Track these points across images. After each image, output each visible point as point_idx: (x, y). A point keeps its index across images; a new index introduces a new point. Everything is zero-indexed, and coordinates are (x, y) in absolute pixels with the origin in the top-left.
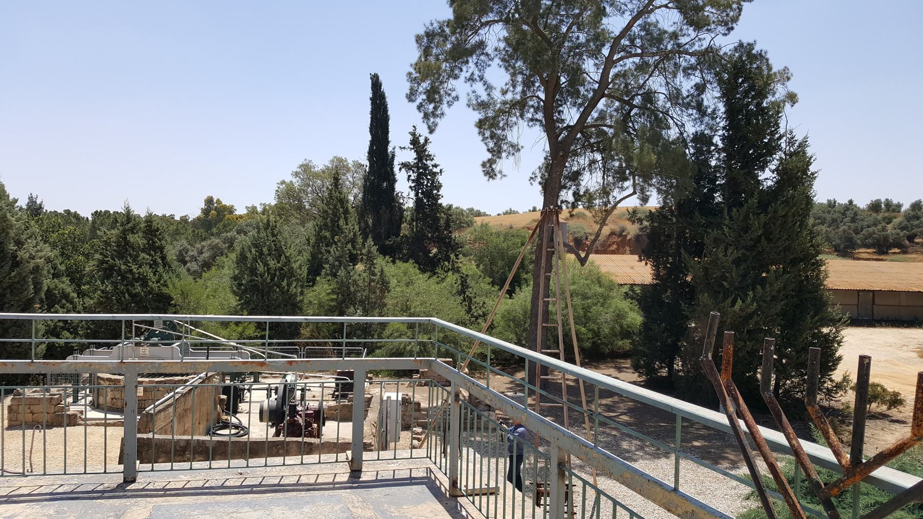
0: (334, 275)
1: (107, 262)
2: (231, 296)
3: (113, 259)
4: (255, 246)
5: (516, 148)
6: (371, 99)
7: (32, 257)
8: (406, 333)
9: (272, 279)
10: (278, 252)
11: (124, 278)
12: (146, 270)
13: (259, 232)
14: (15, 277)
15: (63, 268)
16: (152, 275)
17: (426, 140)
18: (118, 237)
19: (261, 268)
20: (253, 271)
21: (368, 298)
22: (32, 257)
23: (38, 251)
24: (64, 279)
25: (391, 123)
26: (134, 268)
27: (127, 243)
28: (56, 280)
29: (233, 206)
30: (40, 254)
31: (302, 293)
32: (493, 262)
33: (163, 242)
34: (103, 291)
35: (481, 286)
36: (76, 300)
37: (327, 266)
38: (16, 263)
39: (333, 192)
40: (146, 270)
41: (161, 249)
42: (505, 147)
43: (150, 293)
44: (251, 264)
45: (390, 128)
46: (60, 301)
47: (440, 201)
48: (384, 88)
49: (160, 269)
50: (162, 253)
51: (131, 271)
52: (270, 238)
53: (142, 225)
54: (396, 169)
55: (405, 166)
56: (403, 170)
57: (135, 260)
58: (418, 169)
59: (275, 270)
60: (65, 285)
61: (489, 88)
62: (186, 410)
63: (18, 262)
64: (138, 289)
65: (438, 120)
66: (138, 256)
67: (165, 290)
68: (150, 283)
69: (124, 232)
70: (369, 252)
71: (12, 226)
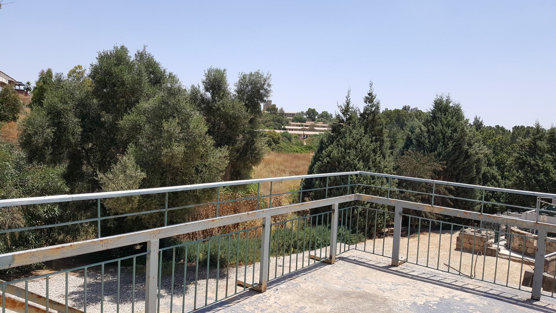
1: (522, 159)
11: (532, 169)
15: (494, 160)
23: (480, 150)
24: (494, 167)
26: (540, 163)
27: (536, 146)
28: (489, 168)
30: (481, 152)
34: (517, 177)
36: (501, 181)
38: (467, 156)
43: (550, 180)
46: (490, 181)
51: (537, 165)
57: (541, 157)
60: (494, 171)
64: (542, 177)
66: (542, 156)
68: (551, 174)
69: (534, 140)
71: (467, 135)
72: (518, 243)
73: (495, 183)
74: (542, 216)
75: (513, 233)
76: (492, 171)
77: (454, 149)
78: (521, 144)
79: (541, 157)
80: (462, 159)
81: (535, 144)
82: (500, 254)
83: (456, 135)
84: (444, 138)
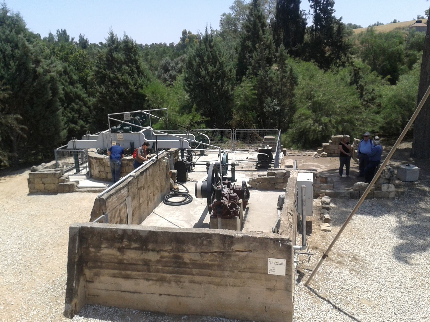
0: (256, 75)
1: (101, 72)
2: (184, 92)
4: (199, 55)
7: (49, 71)
8: (311, 116)
9: (211, 80)
10: (214, 60)
11: (113, 83)
13: (200, 45)
14: (36, 85)
15: (75, 77)
16: (131, 80)
18: (108, 54)
19: (203, 73)
20: (198, 74)
21: (281, 90)
26: (119, 76)
27: (113, 58)
28: (71, 87)
31: (232, 89)
32: (376, 57)
33: (137, 57)
34: (101, 93)
35: (369, 77)
38: (36, 76)
39: (253, 11)
41: (136, 61)
44: (196, 70)
47: (333, 15)
49: (136, 76)
50: (136, 64)
51: (117, 78)
52: (209, 49)
53: (122, 46)
57: (119, 69)
59: (213, 73)
60: (79, 90)
62: (139, 189)
63: (37, 75)
66: (121, 67)
67: (140, 91)
68: (130, 86)
70: (281, 55)
72: (97, 170)
73: (80, 102)
74: (118, 134)
75: (91, 159)
78: (99, 55)
79: (119, 69)
80: (30, 80)
81: (111, 56)
82: (79, 188)
84: (4, 57)
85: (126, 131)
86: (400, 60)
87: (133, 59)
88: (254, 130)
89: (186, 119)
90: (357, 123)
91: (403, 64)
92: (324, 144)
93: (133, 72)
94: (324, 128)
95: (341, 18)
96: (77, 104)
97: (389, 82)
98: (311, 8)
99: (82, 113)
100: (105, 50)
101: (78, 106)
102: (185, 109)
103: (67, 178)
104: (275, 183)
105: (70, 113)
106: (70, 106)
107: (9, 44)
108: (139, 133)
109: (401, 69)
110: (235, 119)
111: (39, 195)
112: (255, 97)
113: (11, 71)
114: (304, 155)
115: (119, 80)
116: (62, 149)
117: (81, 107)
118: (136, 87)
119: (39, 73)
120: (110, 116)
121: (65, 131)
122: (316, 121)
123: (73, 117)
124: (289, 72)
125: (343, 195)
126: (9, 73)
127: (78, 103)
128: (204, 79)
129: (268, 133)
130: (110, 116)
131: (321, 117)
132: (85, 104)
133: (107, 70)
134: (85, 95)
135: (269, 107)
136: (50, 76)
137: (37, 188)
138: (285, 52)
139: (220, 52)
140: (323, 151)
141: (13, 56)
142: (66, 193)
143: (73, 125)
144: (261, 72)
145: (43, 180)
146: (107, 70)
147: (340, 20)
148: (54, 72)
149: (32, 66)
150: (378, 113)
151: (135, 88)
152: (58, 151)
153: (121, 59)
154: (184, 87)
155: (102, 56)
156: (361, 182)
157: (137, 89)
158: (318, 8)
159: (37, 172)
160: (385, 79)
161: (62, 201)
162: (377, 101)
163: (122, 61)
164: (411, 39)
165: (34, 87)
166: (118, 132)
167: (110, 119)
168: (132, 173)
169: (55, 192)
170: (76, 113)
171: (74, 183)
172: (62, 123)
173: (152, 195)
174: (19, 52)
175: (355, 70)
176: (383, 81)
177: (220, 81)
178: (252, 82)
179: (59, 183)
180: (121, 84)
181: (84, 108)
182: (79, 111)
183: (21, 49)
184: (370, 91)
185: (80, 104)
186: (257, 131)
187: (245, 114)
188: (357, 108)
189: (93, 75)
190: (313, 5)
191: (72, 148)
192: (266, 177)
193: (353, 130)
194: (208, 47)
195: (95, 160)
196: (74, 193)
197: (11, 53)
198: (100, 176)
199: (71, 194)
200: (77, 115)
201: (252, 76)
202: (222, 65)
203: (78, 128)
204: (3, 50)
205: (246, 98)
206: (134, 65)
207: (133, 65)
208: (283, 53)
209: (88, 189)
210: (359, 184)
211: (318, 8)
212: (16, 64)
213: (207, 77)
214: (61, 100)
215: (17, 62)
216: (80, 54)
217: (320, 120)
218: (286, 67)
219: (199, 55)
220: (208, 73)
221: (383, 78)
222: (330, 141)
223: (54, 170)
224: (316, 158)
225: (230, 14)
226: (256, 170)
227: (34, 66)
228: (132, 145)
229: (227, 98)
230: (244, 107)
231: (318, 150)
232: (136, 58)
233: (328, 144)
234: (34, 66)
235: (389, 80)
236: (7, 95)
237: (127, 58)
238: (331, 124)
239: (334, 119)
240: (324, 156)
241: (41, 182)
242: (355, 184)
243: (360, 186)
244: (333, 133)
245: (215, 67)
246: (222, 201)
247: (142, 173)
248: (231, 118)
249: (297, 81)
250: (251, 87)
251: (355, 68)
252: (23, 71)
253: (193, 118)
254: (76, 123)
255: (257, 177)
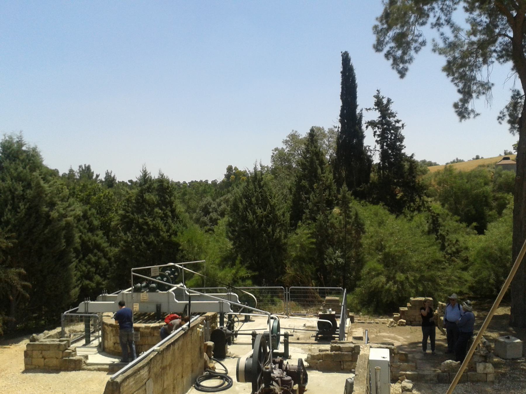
0: (314, 220)
1: (128, 217)
3: (133, 214)
5: (486, 87)
6: (341, 72)
7: (65, 216)
8: (383, 271)
9: (260, 226)
10: (264, 202)
11: (141, 229)
12: (159, 222)
15: (96, 223)
16: (163, 226)
17: (389, 101)
18: (138, 195)
19: (251, 217)
20: (244, 219)
21: (344, 238)
22: (65, 216)
25: (358, 89)
26: (149, 220)
27: (144, 200)
28: (90, 234)
29: (229, 166)
31: (286, 237)
32: (457, 201)
33: (172, 198)
34: (125, 241)
37: (307, 211)
38: (49, 221)
39: (310, 147)
40: (159, 222)
41: (171, 203)
42: (475, 88)
44: (242, 213)
45: (359, 94)
47: (403, 151)
48: (353, 62)
49: (170, 221)
50: (171, 206)
51: (146, 223)
52: (258, 189)
53: (156, 185)
54: (364, 127)
55: (372, 124)
56: (370, 127)
57: (151, 213)
58: (383, 125)
59: (262, 218)
60: (99, 238)
61: (456, 30)
65: (407, 65)
66: (152, 210)
67: (174, 239)
68: (161, 233)
70: (344, 197)
72: (112, 341)
73: (99, 253)
74: (142, 294)
75: (106, 327)
76: (95, 238)
77: (28, 213)
78: (127, 196)
79: (151, 213)
81: (142, 197)
82: (88, 365)
83: (30, 193)
84: (13, 198)
85: (152, 290)
86: (487, 204)
87: (167, 200)
88: (313, 289)
89: (227, 274)
90: (440, 282)
91: (491, 210)
92: (402, 309)
93: (166, 216)
94: (400, 287)
95: (413, 155)
96: (95, 256)
97: (476, 232)
98: (376, 144)
99: (100, 267)
100: (135, 191)
101: (97, 258)
102: (227, 260)
103: (73, 351)
104: (340, 362)
105: (86, 266)
106: (86, 258)
107: (21, 183)
108: (169, 293)
109: (489, 215)
110: (289, 274)
111: (37, 372)
112: (313, 246)
113: (19, 214)
114: (377, 323)
115: (148, 225)
116: (70, 312)
117: (99, 258)
118: (169, 234)
119: (53, 218)
120: (134, 271)
121: (77, 289)
122: (389, 279)
123: (89, 272)
124: (354, 217)
125: (428, 378)
126: (17, 217)
127: (96, 253)
128: (251, 225)
129: (330, 293)
130: (134, 271)
131: (395, 274)
132: (105, 255)
133: (135, 214)
134: (105, 245)
135: (331, 259)
136: (66, 221)
137: (34, 364)
138: (348, 194)
139: (271, 192)
140: (400, 318)
141: (23, 197)
142: (71, 371)
143: (87, 282)
144: (320, 217)
145: (44, 353)
146: (135, 214)
147: (412, 157)
148: (71, 216)
149: (45, 209)
150: (465, 269)
151: (168, 236)
152: (65, 316)
153: (153, 201)
154: (227, 233)
155: (131, 197)
156: (451, 361)
157: (170, 236)
158: (385, 144)
159: (37, 343)
160: (470, 227)
161: (65, 382)
162: (463, 254)
163: (154, 203)
164: (498, 180)
165: (44, 234)
166: (143, 290)
167: (134, 275)
168: (156, 347)
169: (56, 370)
170: (92, 267)
171: (82, 358)
172: (74, 279)
173: (180, 376)
174: (32, 192)
175: (433, 216)
176: (468, 230)
177: (271, 227)
178: (310, 229)
179: (62, 358)
180: (151, 230)
181: (103, 261)
182: (96, 264)
183: (33, 189)
184: (454, 242)
185: (98, 255)
186: (316, 289)
187: (301, 268)
188: (439, 262)
189: (118, 220)
190: (380, 140)
191: (83, 311)
192: (329, 352)
193: (436, 290)
194: (257, 187)
195: (111, 328)
196: (81, 371)
197: (21, 193)
198: (115, 349)
199: (77, 372)
200: (93, 269)
201: (310, 222)
202: (273, 207)
203: (94, 285)
204: (13, 190)
205: (302, 247)
206: (169, 208)
207: (167, 207)
208: (347, 195)
209: (99, 367)
210: (447, 363)
211: (385, 144)
212: (26, 207)
213: (255, 222)
214: (76, 250)
215: (28, 204)
216: (105, 194)
217: (394, 278)
218: (350, 211)
219: (246, 196)
220: (257, 217)
221: (468, 226)
222: (409, 305)
223: (58, 340)
224: (393, 326)
225: (282, 148)
226: (316, 342)
227: (47, 209)
228: (158, 307)
229: (279, 248)
230: (300, 259)
231: (395, 316)
232: (171, 200)
233: (406, 309)
234: (47, 209)
235: (476, 228)
236: (10, 245)
237: (161, 200)
238: (409, 282)
239: (411, 276)
240: (401, 324)
241: (41, 356)
242: (442, 364)
243: (450, 365)
244: (412, 295)
245: (265, 211)
246: (272, 387)
247: (169, 347)
248: (284, 273)
249: (364, 229)
250: (308, 234)
251: (433, 214)
252: (34, 215)
253: (237, 273)
254: (91, 279)
255: (317, 353)
